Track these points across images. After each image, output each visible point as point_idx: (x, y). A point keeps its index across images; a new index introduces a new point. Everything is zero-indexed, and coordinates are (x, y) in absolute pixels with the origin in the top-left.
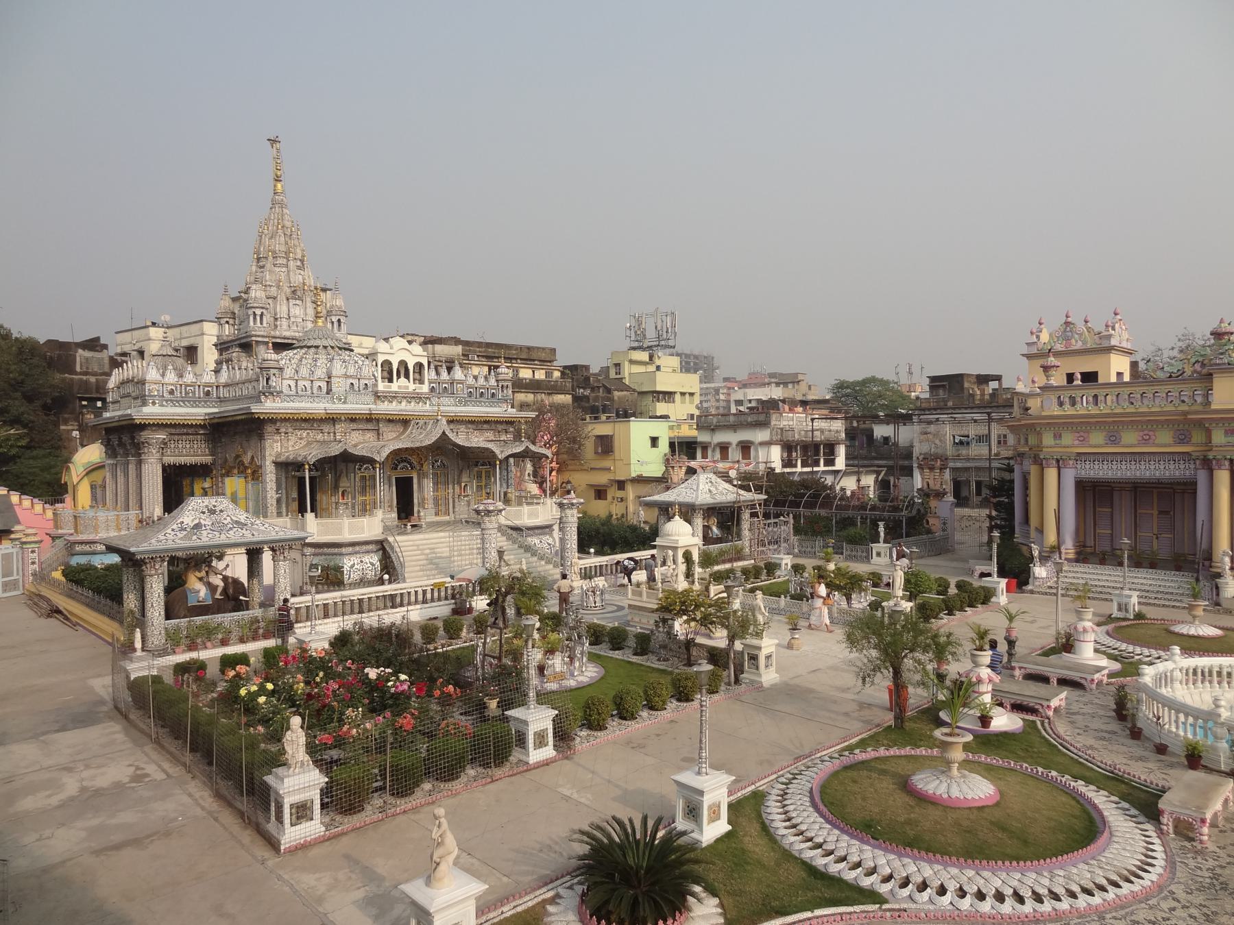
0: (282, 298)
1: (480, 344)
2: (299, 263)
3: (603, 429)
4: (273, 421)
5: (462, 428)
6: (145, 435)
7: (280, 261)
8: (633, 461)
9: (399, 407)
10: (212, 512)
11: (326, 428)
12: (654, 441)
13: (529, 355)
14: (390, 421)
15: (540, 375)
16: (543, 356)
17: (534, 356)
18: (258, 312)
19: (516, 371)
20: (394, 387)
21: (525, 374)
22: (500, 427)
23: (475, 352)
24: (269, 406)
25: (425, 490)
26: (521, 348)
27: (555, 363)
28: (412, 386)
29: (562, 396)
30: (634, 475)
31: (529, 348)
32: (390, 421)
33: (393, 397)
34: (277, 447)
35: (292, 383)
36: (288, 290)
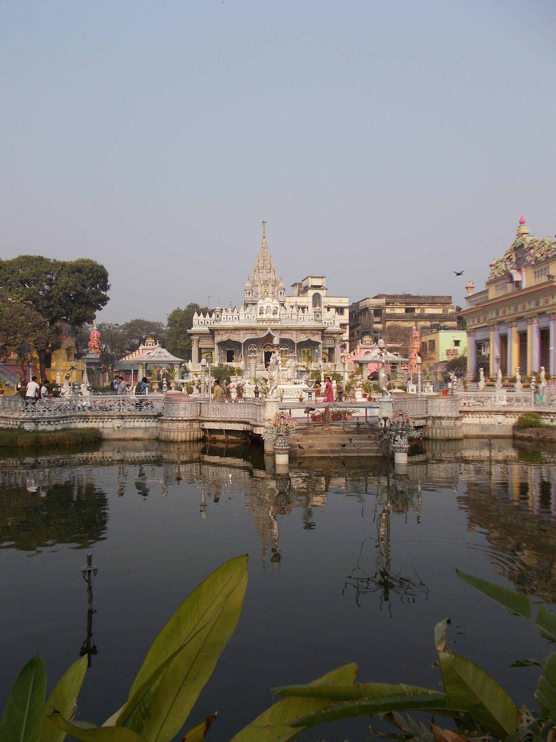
0: (259, 285)
1: (401, 297)
2: (268, 270)
3: (431, 337)
4: (217, 330)
5: (295, 332)
6: (192, 337)
7: (260, 271)
8: (440, 353)
9: (266, 324)
10: (160, 353)
11: (237, 332)
12: (457, 343)
13: (433, 301)
14: (261, 330)
15: (438, 311)
16: (443, 301)
17: (436, 301)
18: (248, 292)
19: (423, 309)
20: (264, 316)
21: (429, 311)
22: (314, 332)
23: (398, 301)
24: (217, 325)
25: (276, 356)
26: (428, 298)
27: (451, 305)
28: (272, 317)
29: (451, 323)
30: (441, 360)
31: (433, 297)
32: (261, 330)
33: (263, 321)
34: (218, 339)
35: (225, 317)
36: (262, 282)
